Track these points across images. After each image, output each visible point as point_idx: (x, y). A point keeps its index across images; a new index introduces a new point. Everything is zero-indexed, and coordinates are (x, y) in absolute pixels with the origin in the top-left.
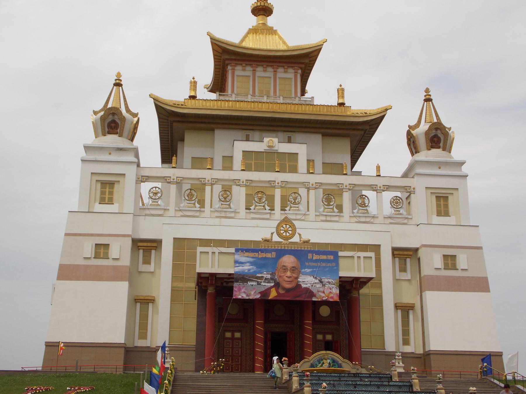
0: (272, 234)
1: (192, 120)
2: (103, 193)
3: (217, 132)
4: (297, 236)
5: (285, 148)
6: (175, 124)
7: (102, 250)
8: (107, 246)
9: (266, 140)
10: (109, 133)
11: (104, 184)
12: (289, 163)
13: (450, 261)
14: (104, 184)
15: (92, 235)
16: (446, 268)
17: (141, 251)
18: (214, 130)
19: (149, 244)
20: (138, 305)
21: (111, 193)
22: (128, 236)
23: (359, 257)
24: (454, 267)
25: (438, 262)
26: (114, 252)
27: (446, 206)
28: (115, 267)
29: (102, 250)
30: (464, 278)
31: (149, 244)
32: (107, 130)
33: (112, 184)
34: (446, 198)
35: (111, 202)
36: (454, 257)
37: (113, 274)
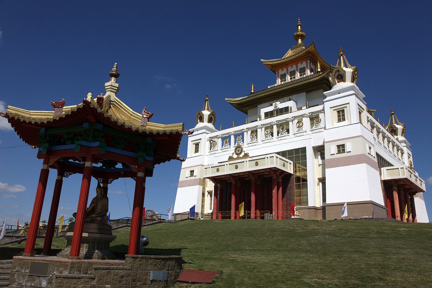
0: (233, 153)
3: (258, 106)
4: (243, 152)
5: (280, 105)
9: (274, 104)
10: (200, 122)
12: (286, 110)
13: (341, 148)
16: (339, 152)
18: (257, 106)
23: (267, 158)
24: (344, 151)
25: (334, 150)
27: (344, 115)
30: (349, 157)
34: (343, 111)
36: (343, 146)
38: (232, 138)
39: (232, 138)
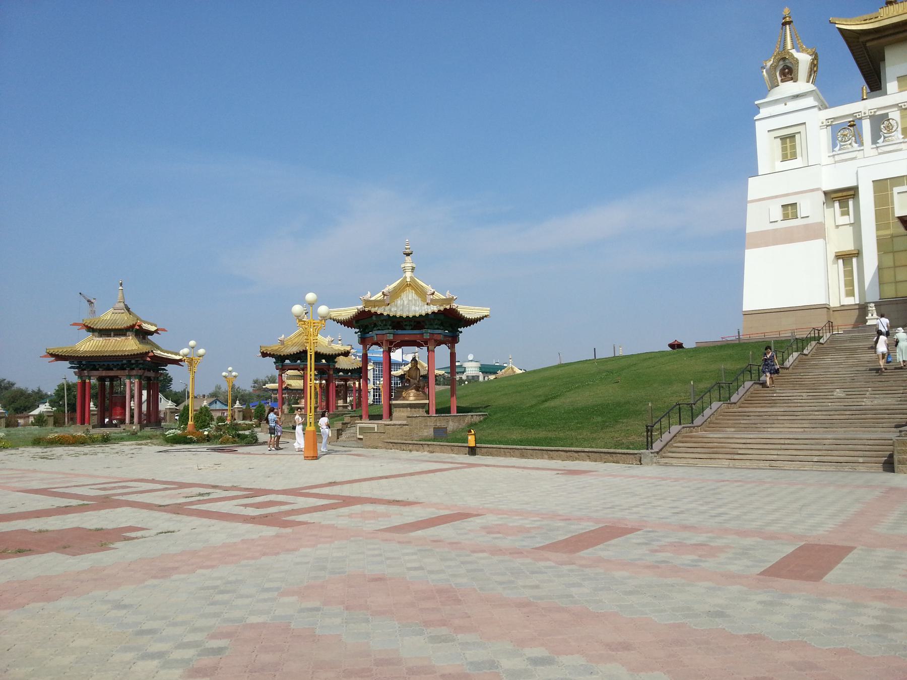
1: (891, 32)
2: (784, 149)
6: (868, 44)
7: (790, 210)
8: (794, 205)
10: (783, 81)
11: (783, 139)
14: (783, 139)
15: (776, 197)
17: (837, 204)
19: (845, 194)
20: (840, 261)
21: (794, 147)
22: (818, 189)
26: (803, 210)
28: (806, 226)
29: (790, 210)
31: (845, 194)
32: (779, 79)
33: (792, 137)
35: (794, 156)
37: (816, 232)
38: (866, 125)
39: (866, 125)
